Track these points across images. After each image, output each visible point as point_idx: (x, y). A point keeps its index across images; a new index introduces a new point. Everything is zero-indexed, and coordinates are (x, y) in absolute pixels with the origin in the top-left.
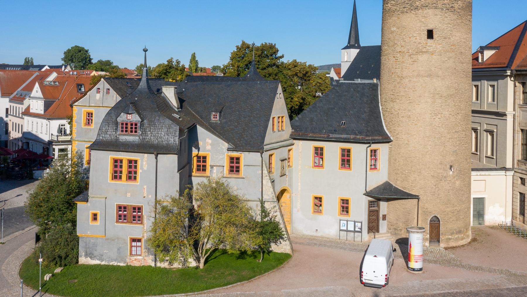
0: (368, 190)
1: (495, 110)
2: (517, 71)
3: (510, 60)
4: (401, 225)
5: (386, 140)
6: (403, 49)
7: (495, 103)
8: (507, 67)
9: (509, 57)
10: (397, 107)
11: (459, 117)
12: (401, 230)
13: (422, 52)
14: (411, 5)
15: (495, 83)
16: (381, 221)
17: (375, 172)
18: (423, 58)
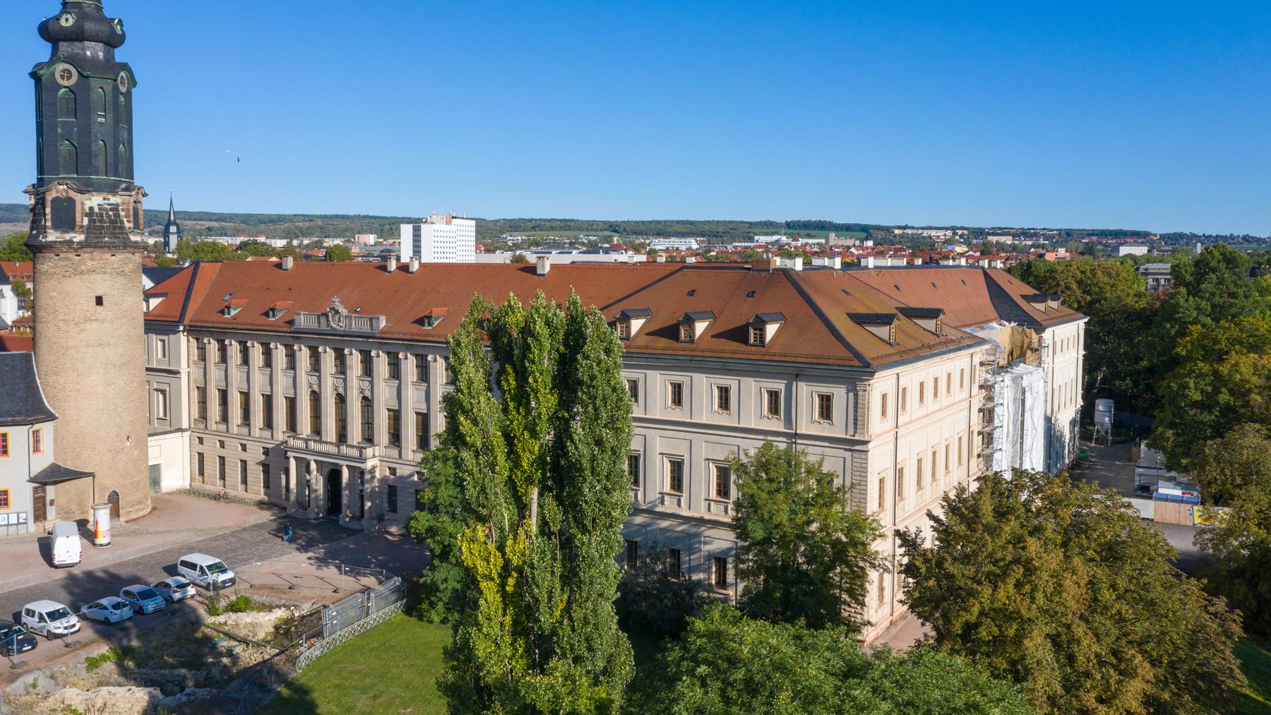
0: (32, 476)
1: (167, 367)
2: (190, 326)
3: (181, 313)
4: (74, 507)
5: (50, 417)
6: (66, 317)
7: (167, 359)
8: (179, 322)
9: (180, 309)
10: (62, 381)
11: (135, 385)
12: (74, 513)
13: (91, 320)
14: (75, 269)
15: (165, 338)
16: (48, 508)
17: (38, 454)
18: (91, 327)
